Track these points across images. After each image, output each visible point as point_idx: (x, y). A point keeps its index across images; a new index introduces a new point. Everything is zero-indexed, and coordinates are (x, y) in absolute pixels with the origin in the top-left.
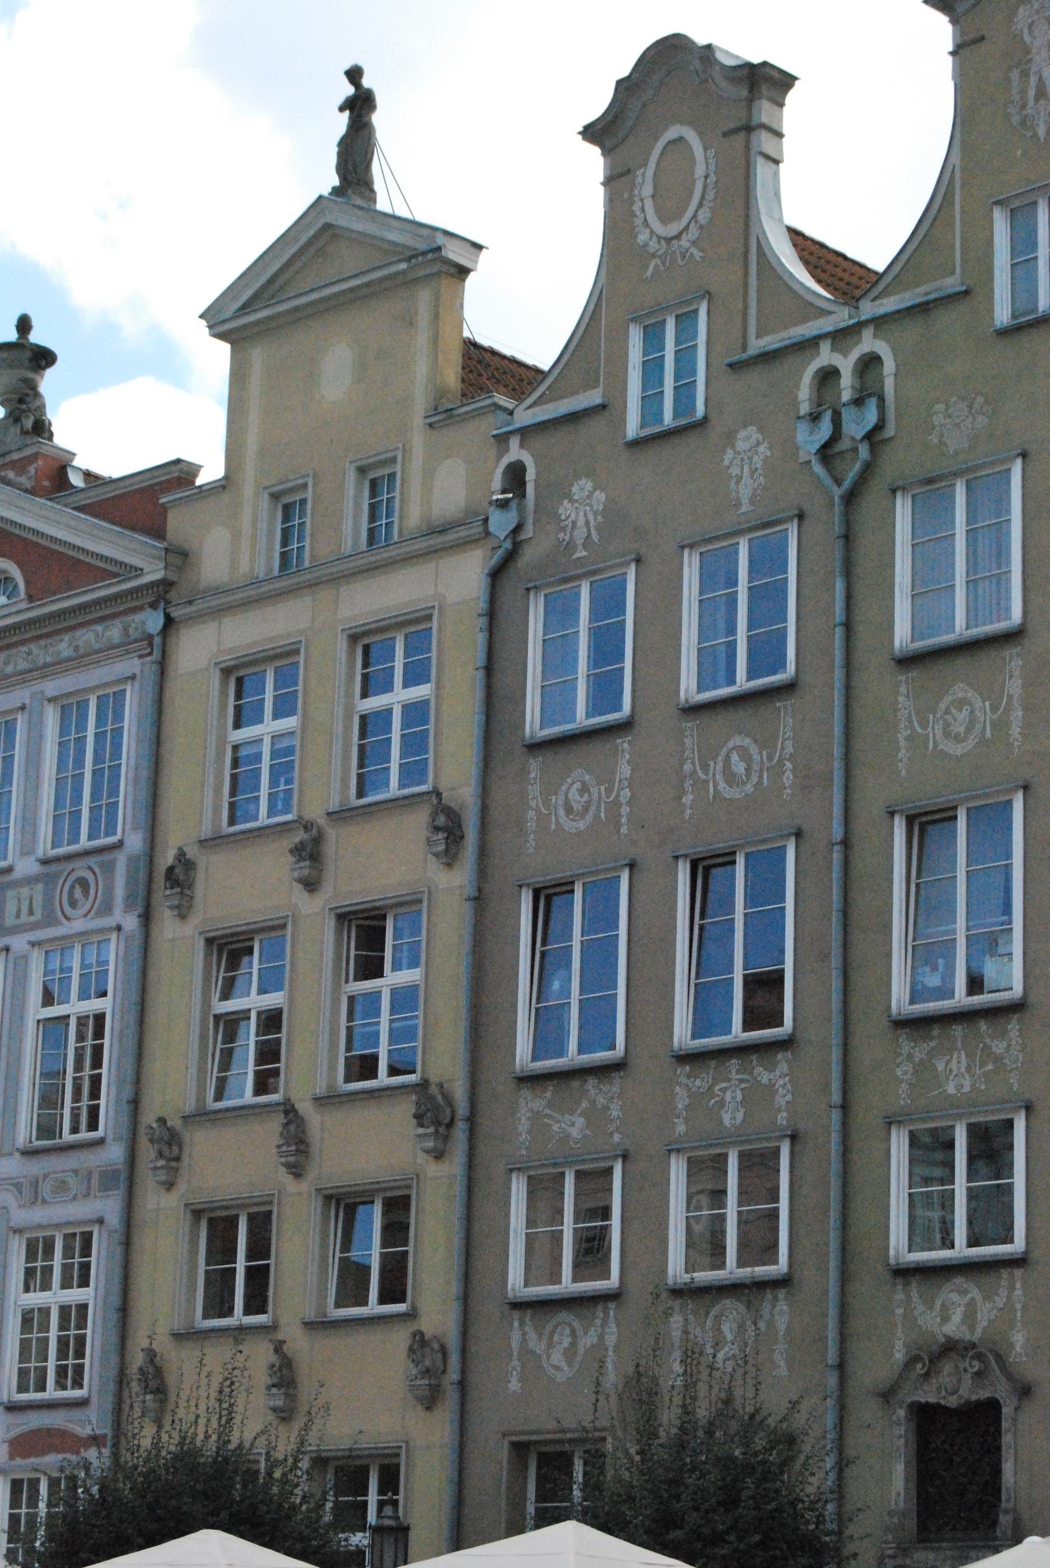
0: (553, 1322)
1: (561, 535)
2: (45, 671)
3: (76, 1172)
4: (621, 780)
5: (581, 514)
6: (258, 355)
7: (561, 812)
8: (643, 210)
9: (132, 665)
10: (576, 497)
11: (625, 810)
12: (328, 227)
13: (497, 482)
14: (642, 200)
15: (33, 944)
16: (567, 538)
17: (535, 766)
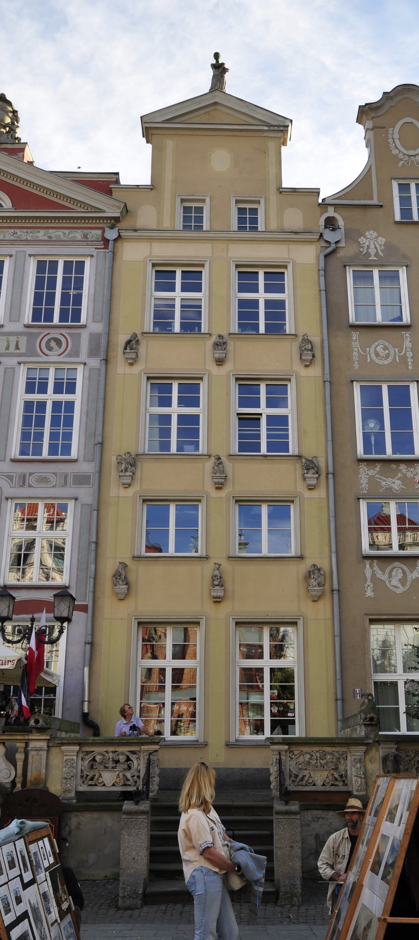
0: (390, 567)
1: (361, 249)
2: (27, 242)
3: (55, 474)
4: (406, 348)
5: (372, 244)
6: (170, 144)
7: (373, 355)
8: (394, 142)
9: (92, 250)
10: (368, 237)
11: (410, 360)
12: (216, 103)
13: (322, 222)
14: (393, 139)
15: (19, 363)
16: (365, 251)
17: (355, 335)
